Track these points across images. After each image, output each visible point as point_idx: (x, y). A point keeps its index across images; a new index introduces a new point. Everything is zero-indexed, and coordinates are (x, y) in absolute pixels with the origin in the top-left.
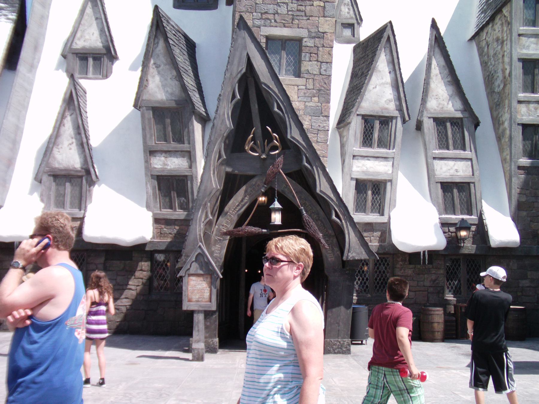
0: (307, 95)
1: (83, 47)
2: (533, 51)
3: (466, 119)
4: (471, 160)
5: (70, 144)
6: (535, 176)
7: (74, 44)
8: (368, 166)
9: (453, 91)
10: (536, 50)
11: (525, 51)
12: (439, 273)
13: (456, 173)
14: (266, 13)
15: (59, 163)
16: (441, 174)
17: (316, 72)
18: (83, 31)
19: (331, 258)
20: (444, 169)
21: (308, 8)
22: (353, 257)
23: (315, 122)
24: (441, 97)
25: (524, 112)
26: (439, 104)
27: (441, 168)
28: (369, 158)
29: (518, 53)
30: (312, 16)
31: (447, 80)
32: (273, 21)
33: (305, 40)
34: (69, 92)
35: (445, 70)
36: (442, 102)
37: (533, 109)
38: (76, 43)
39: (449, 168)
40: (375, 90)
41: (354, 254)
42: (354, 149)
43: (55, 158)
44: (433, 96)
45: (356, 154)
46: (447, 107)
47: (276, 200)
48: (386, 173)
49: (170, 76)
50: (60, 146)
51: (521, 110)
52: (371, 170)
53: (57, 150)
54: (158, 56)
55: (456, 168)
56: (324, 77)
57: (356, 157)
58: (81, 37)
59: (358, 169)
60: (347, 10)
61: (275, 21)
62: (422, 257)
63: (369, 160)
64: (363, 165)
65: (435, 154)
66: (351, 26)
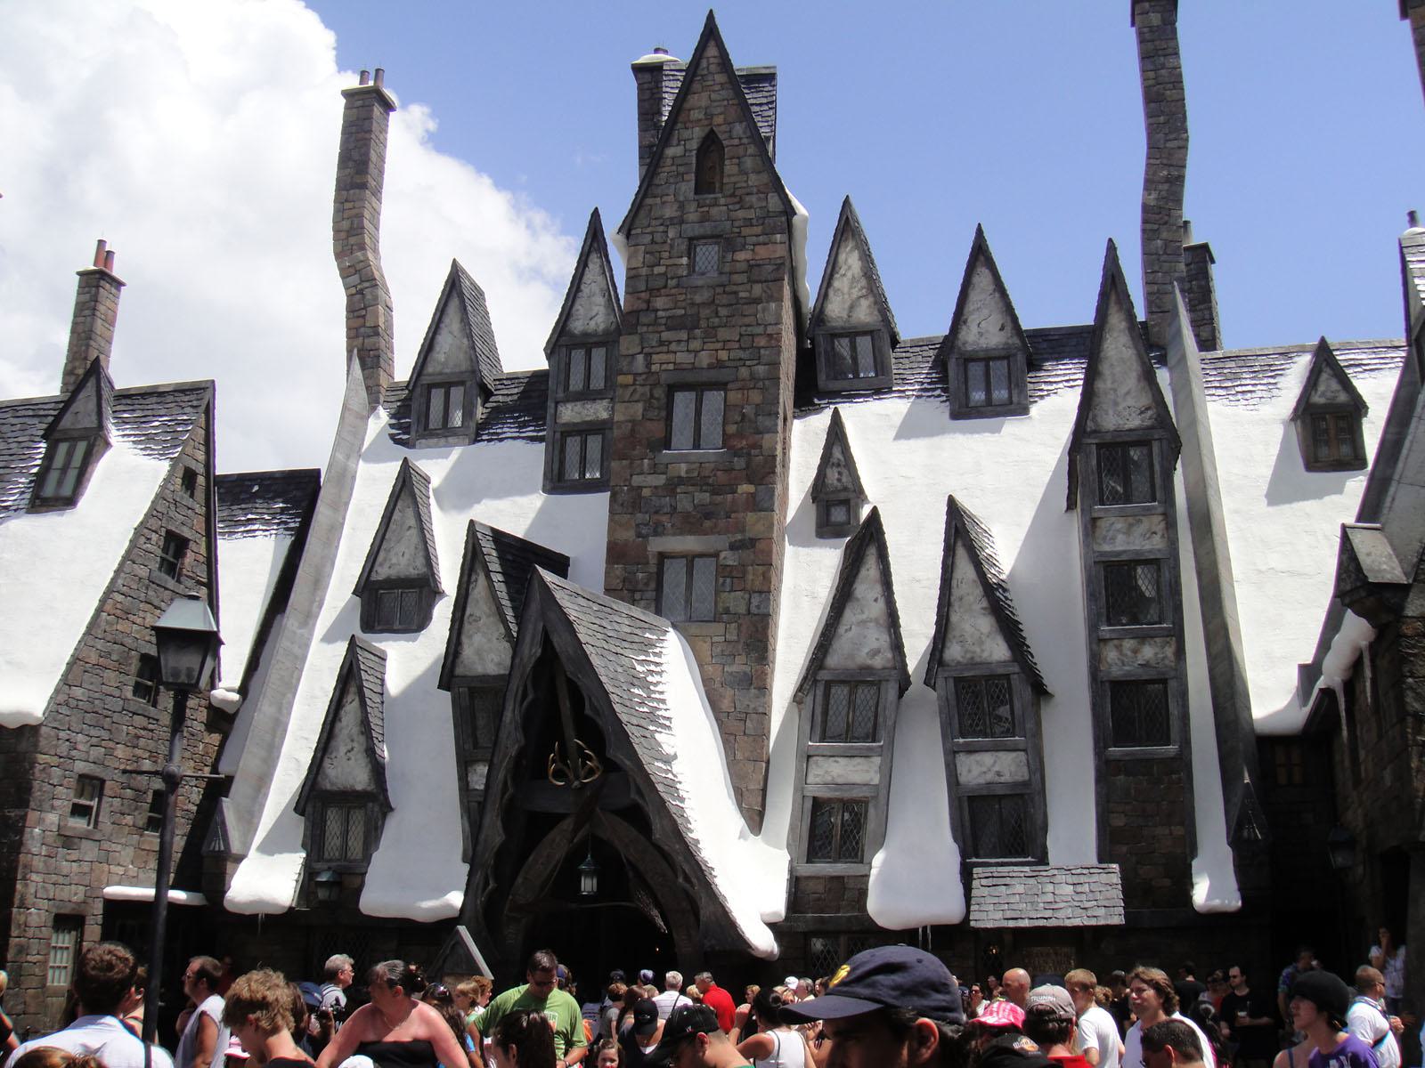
3: (1016, 676)
5: (349, 751)
6: (1141, 778)
7: (373, 574)
8: (834, 774)
9: (992, 626)
10: (1128, 543)
11: (1106, 548)
13: (997, 779)
15: (332, 784)
17: (742, 610)
18: (388, 551)
20: (976, 771)
21: (730, 496)
24: (969, 640)
26: (966, 652)
27: (970, 771)
28: (837, 759)
29: (1094, 552)
31: (980, 606)
33: (723, 555)
34: (347, 665)
37: (1129, 653)
39: (984, 769)
40: (850, 634)
41: (713, 942)
43: (327, 776)
44: (954, 637)
49: (496, 635)
50: (333, 756)
53: (330, 761)
54: (477, 601)
55: (996, 768)
56: (754, 618)
57: (815, 758)
58: (385, 560)
59: (818, 780)
60: (836, 476)
62: (920, 938)
63: (837, 762)
64: (827, 772)
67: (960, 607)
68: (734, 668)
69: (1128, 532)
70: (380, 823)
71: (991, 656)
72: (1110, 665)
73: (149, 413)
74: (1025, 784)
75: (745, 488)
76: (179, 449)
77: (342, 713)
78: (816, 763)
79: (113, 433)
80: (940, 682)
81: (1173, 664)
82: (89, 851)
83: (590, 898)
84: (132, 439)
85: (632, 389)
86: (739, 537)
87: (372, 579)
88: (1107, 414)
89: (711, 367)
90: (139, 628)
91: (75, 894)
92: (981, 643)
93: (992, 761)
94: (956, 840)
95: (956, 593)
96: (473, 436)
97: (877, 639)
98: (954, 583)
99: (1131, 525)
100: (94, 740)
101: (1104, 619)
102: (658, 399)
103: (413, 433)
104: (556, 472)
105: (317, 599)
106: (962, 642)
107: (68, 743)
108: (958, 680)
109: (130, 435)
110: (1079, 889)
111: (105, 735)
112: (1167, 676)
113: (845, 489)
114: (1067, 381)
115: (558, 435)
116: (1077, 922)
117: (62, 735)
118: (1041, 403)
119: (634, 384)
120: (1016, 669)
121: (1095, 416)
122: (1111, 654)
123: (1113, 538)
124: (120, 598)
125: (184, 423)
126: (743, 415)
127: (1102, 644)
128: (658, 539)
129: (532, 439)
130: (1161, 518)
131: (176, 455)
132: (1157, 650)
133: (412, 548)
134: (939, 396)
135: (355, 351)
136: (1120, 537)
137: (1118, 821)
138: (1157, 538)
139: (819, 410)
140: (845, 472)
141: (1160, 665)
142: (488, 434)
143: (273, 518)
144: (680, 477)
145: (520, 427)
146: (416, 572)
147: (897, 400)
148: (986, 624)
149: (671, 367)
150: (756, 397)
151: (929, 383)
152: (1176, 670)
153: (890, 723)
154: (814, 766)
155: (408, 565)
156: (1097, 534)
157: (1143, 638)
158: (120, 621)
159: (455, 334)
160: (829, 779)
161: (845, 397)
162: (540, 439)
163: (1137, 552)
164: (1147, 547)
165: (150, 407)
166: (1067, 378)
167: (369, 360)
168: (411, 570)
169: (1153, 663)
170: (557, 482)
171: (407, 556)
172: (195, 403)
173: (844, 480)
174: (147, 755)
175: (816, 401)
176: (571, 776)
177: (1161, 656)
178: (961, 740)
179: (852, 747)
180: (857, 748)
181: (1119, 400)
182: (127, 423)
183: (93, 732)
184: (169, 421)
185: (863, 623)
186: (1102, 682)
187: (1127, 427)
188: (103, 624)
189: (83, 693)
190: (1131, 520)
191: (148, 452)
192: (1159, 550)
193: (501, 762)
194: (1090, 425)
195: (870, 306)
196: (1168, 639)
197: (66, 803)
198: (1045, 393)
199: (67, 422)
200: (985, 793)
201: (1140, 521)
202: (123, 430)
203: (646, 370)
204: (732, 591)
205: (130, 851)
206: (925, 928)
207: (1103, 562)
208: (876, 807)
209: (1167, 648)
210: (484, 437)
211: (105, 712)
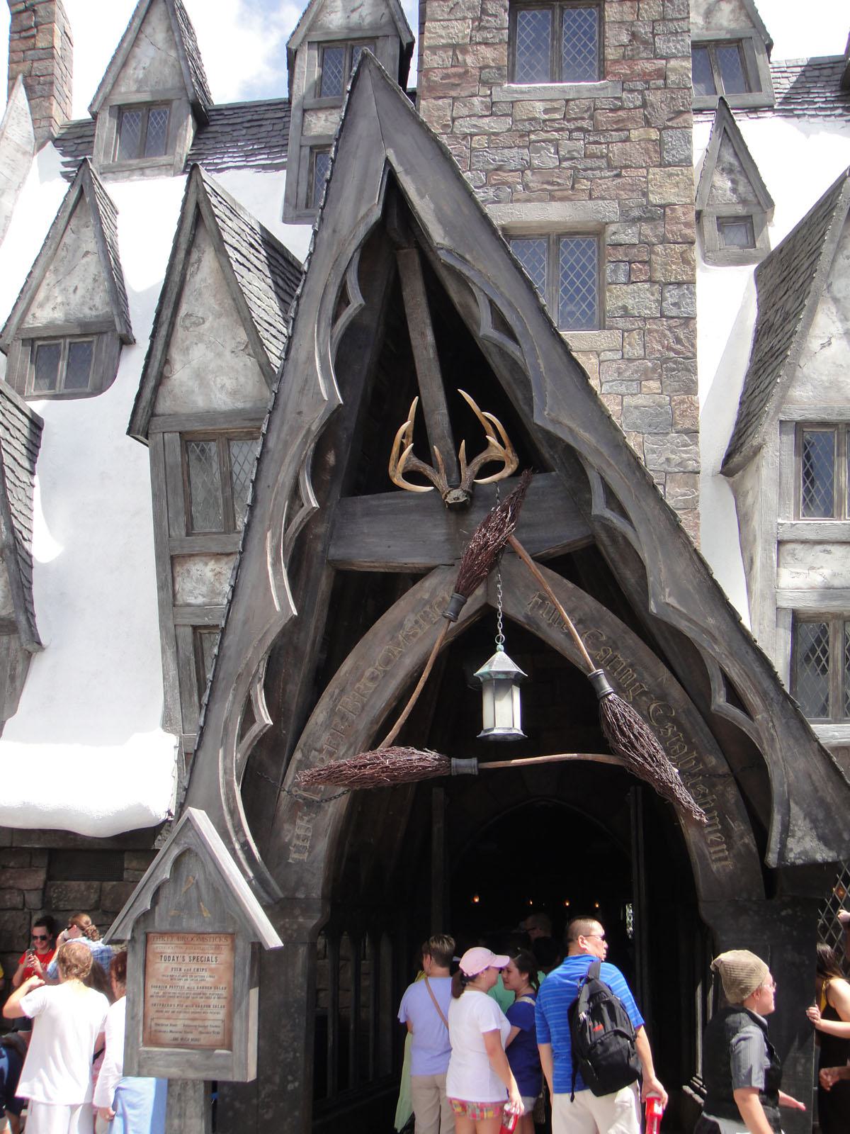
1: (50, 323)
7: (29, 318)
14: (499, 169)
19: (720, 859)
21: (616, 148)
22: (805, 852)
23: (653, 452)
28: (829, 547)
30: (626, 167)
32: (520, 187)
38: (34, 315)
40: (828, 352)
45: (786, 537)
47: (500, 646)
49: (231, 344)
56: (673, 323)
57: (789, 547)
58: (47, 298)
61: (526, 187)
63: (829, 552)
68: (640, 400)
70: (20, 668)
78: (793, 555)
83: (505, 746)
87: (26, 326)
104: (302, 196)
115: (306, 151)
133: (90, 280)
145: (247, 156)
146: (94, 313)
151: (823, 102)
154: (789, 558)
155: (83, 304)
159: (160, 45)
162: (277, 167)
168: (87, 311)
171: (80, 292)
173: (741, 189)
193: (286, 445)
195: (733, 11)
204: (630, 282)
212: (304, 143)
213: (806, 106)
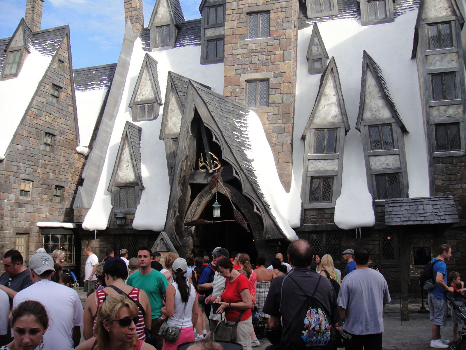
0: (274, 119)
1: (141, 100)
2: (439, 66)
3: (394, 124)
4: (399, 154)
5: (127, 166)
6: (449, 164)
7: (136, 99)
8: (319, 166)
9: (383, 104)
10: (442, 65)
11: (432, 68)
12: (375, 244)
13: (387, 167)
15: (121, 179)
16: (375, 168)
17: (280, 101)
18: (141, 90)
19: (259, 238)
20: (378, 164)
21: (273, 56)
22: (269, 237)
23: (280, 138)
24: (374, 110)
25: (435, 115)
26: (373, 115)
27: (375, 164)
28: (320, 161)
29: (427, 70)
32: (249, 69)
33: (271, 80)
34: (125, 133)
35: (377, 88)
36: (375, 113)
37: (443, 112)
38: (137, 98)
40: (324, 109)
41: (269, 236)
42: (309, 154)
43: (119, 176)
45: (310, 159)
46: (379, 116)
47: (217, 201)
48: (333, 171)
50: (121, 168)
51: (433, 113)
52: (322, 169)
53: (120, 170)
54: (173, 104)
55: (387, 162)
58: (140, 93)
59: (312, 169)
60: (316, 49)
61: (250, 69)
62: (357, 233)
63: (320, 162)
64: (316, 166)
65: (370, 153)
66: (320, 60)
67: (369, 96)
68: (277, 125)
69: (441, 61)
70: (140, 194)
71: (383, 116)
72: (435, 117)
73: (45, 39)
74: (399, 169)
75: (279, 52)
76: (56, 52)
77: (124, 152)
79: (32, 49)
80: (362, 128)
81: (462, 116)
82: (29, 208)
83: (217, 218)
84: (39, 50)
85: (232, 15)
86: (277, 72)
87: (136, 101)
88: (431, 11)
89: (263, 4)
90: (43, 122)
91: (27, 225)
92: (379, 111)
93: (385, 160)
94: (370, 192)
95: (368, 90)
96: (174, 45)
97: (335, 111)
98: (367, 86)
99: (442, 58)
100: (27, 166)
101: (432, 97)
102: (243, 19)
103: (151, 46)
104: (205, 56)
105: (116, 110)
106: (371, 111)
107: (16, 167)
108: (370, 126)
109: (37, 49)
110: (435, 207)
111: (33, 164)
112: (459, 121)
113: (320, 54)
114: (410, 8)
115: (206, 42)
116: (436, 222)
117: (14, 163)
118: (399, 17)
119: (233, 14)
120: (393, 121)
121: (426, 12)
122: (435, 112)
123: (435, 64)
124: (35, 110)
125: (58, 42)
126: (277, 23)
127: (431, 108)
128: (245, 75)
129: (196, 45)
130: (456, 54)
131: (54, 54)
132: (455, 110)
134: (357, 17)
135: (128, 17)
136: (438, 63)
137: (439, 183)
138: (454, 63)
139: (308, 25)
140: (320, 47)
141: (456, 117)
142: (179, 44)
143: (101, 82)
144: (253, 49)
145: (191, 41)
147: (340, 20)
148: (381, 103)
149: (247, 5)
150: (282, 15)
151: (352, 13)
152: (463, 118)
153: (341, 145)
155: (149, 94)
156: (428, 62)
157: (449, 105)
158: (35, 119)
160: (317, 169)
161: (319, 20)
162: (199, 44)
163: (445, 69)
164: (450, 67)
165: (45, 37)
166: (409, 7)
167: (133, 20)
169: (453, 116)
170: (206, 59)
172: (61, 34)
173: (319, 50)
174: (51, 171)
175: (307, 22)
176: (209, 168)
177: (457, 113)
178: (371, 151)
179: (326, 155)
180: (328, 156)
181: (437, 5)
182: (37, 44)
183: (27, 162)
184: (52, 42)
185: (329, 104)
186: (431, 124)
187: (440, 16)
188: (28, 120)
189: (21, 148)
190: (443, 55)
191: (44, 54)
192: (455, 68)
193: (179, 163)
194: (424, 16)
196: (460, 105)
197: (17, 190)
198: (400, 13)
199: (13, 45)
200: (382, 173)
201: (447, 56)
202: (35, 47)
203: (237, 8)
205: (47, 209)
206: (358, 229)
207: (431, 74)
208: (337, 180)
209: (459, 109)
210: (178, 45)
211: (32, 155)
212: (205, 39)
213: (347, 14)
